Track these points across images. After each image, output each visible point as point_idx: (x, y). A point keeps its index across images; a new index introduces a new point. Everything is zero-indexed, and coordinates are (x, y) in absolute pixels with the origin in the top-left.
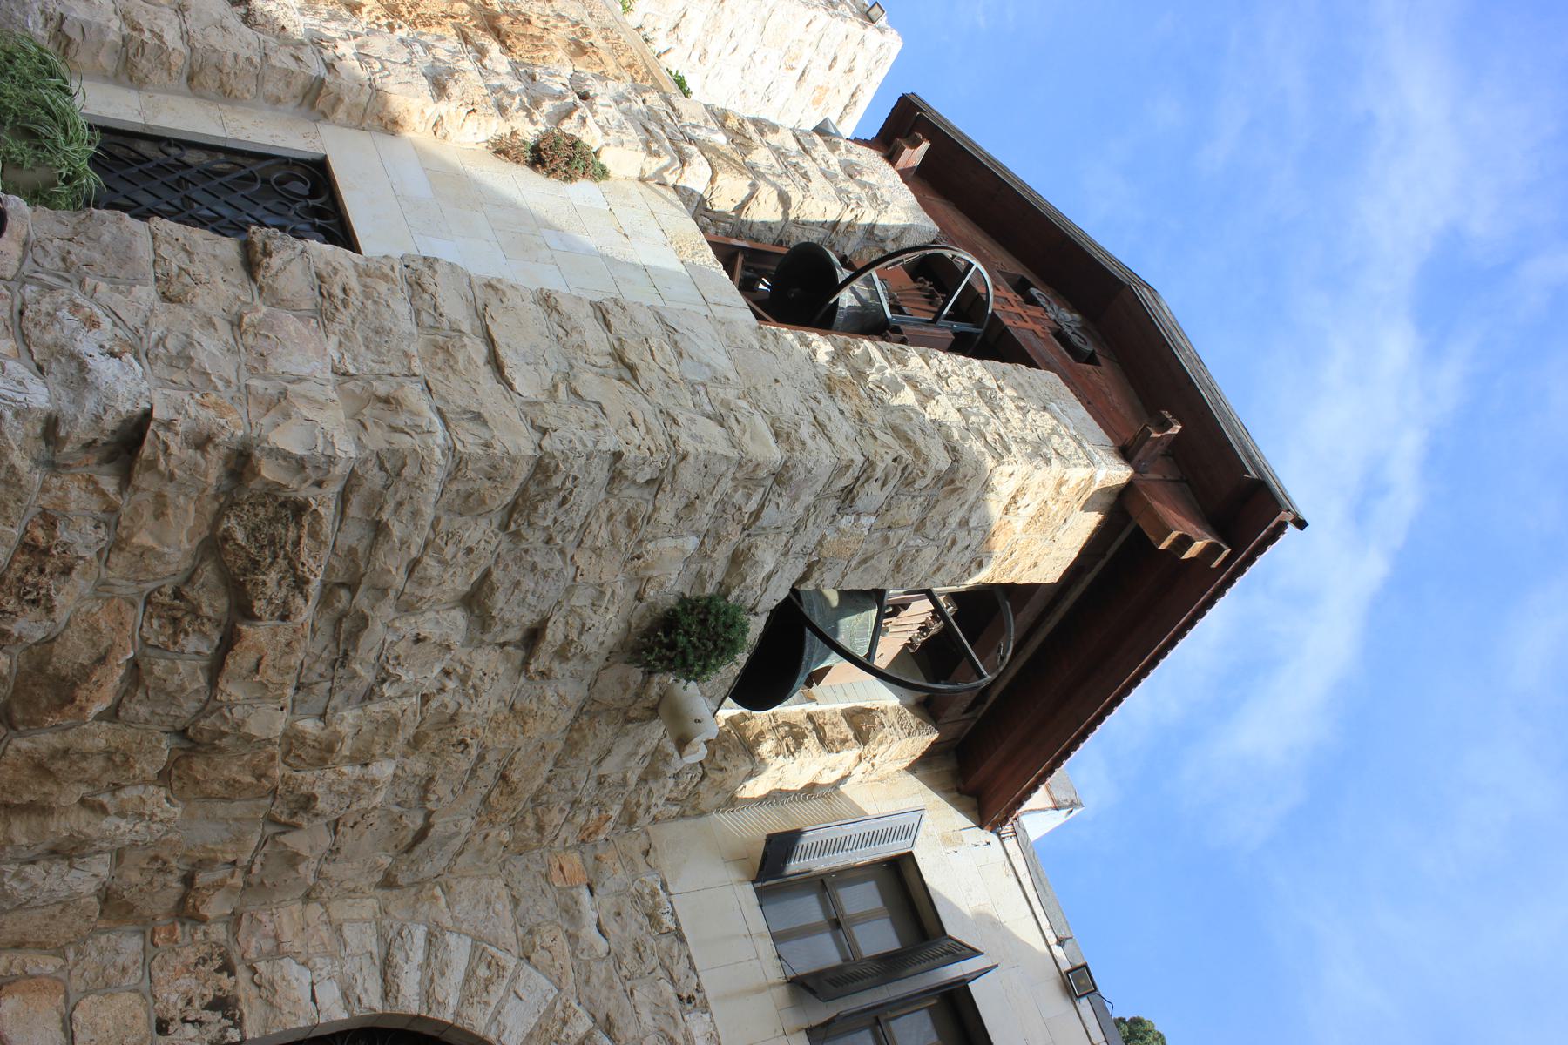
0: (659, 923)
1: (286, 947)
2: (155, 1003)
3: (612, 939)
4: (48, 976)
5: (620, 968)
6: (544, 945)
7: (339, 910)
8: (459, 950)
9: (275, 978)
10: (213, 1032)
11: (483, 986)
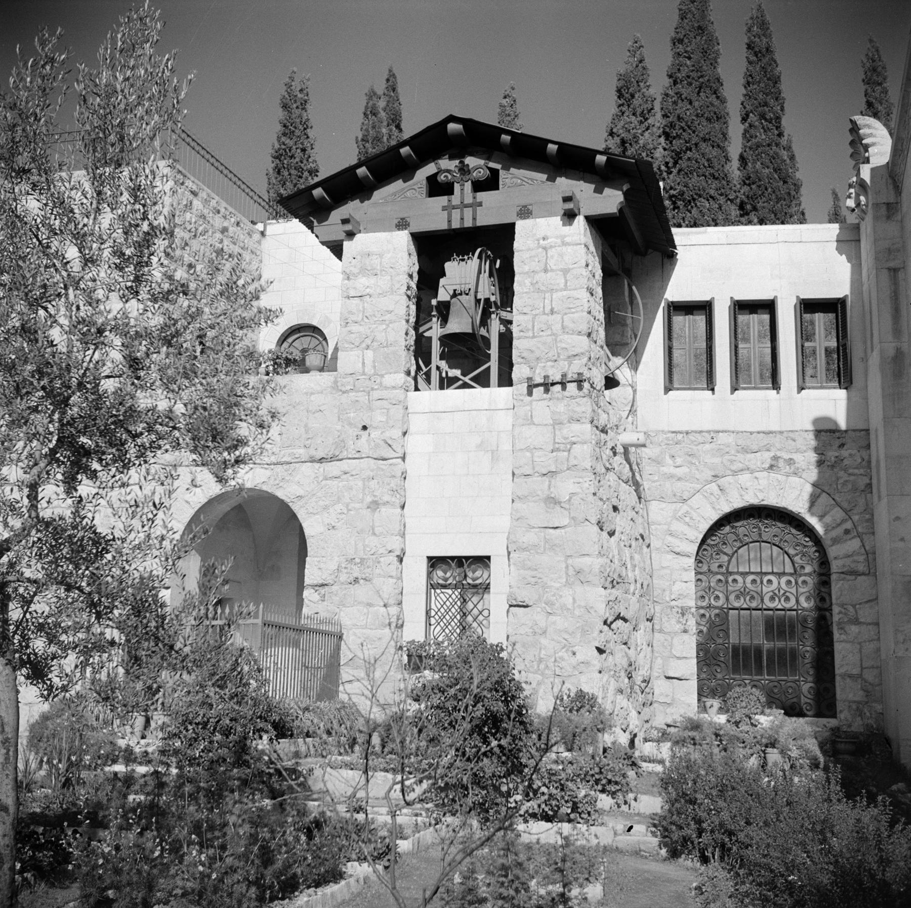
8: (677, 526)
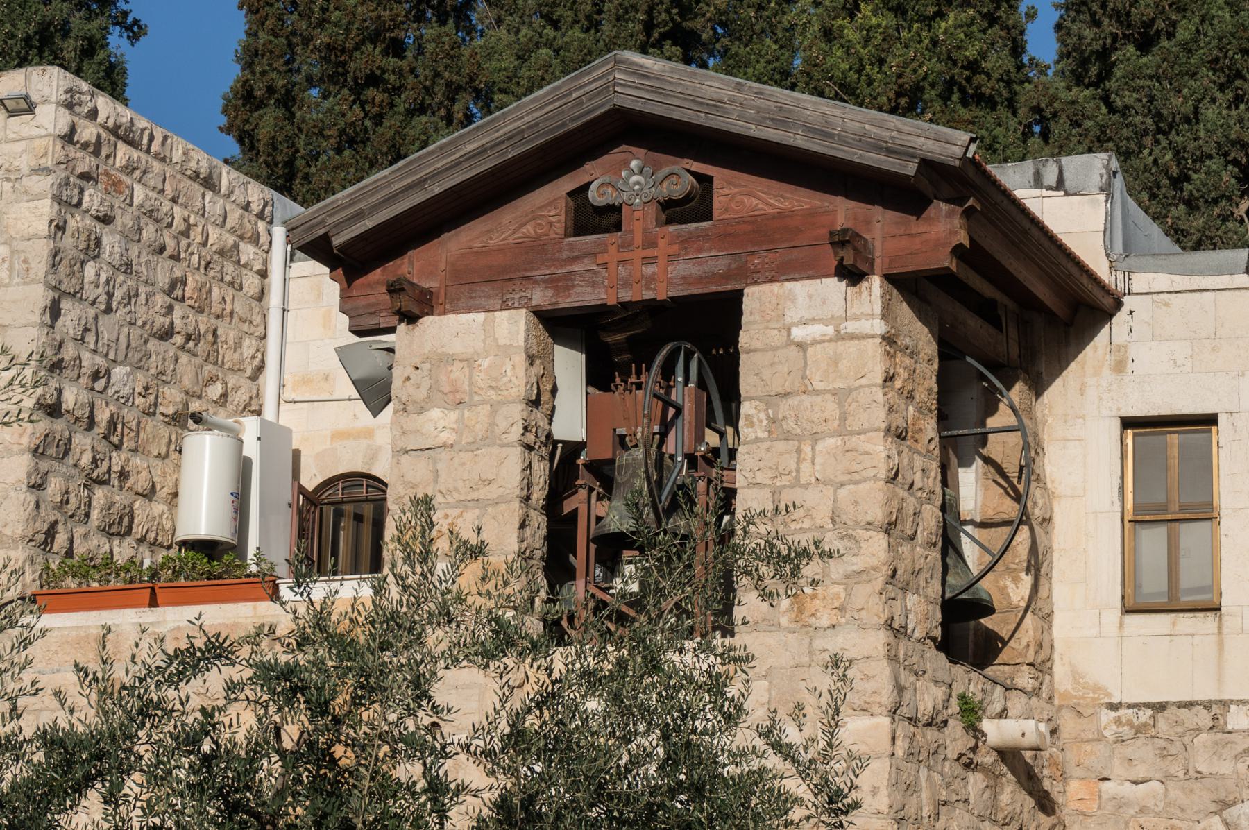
0: (1145, 725)
3: (1151, 775)
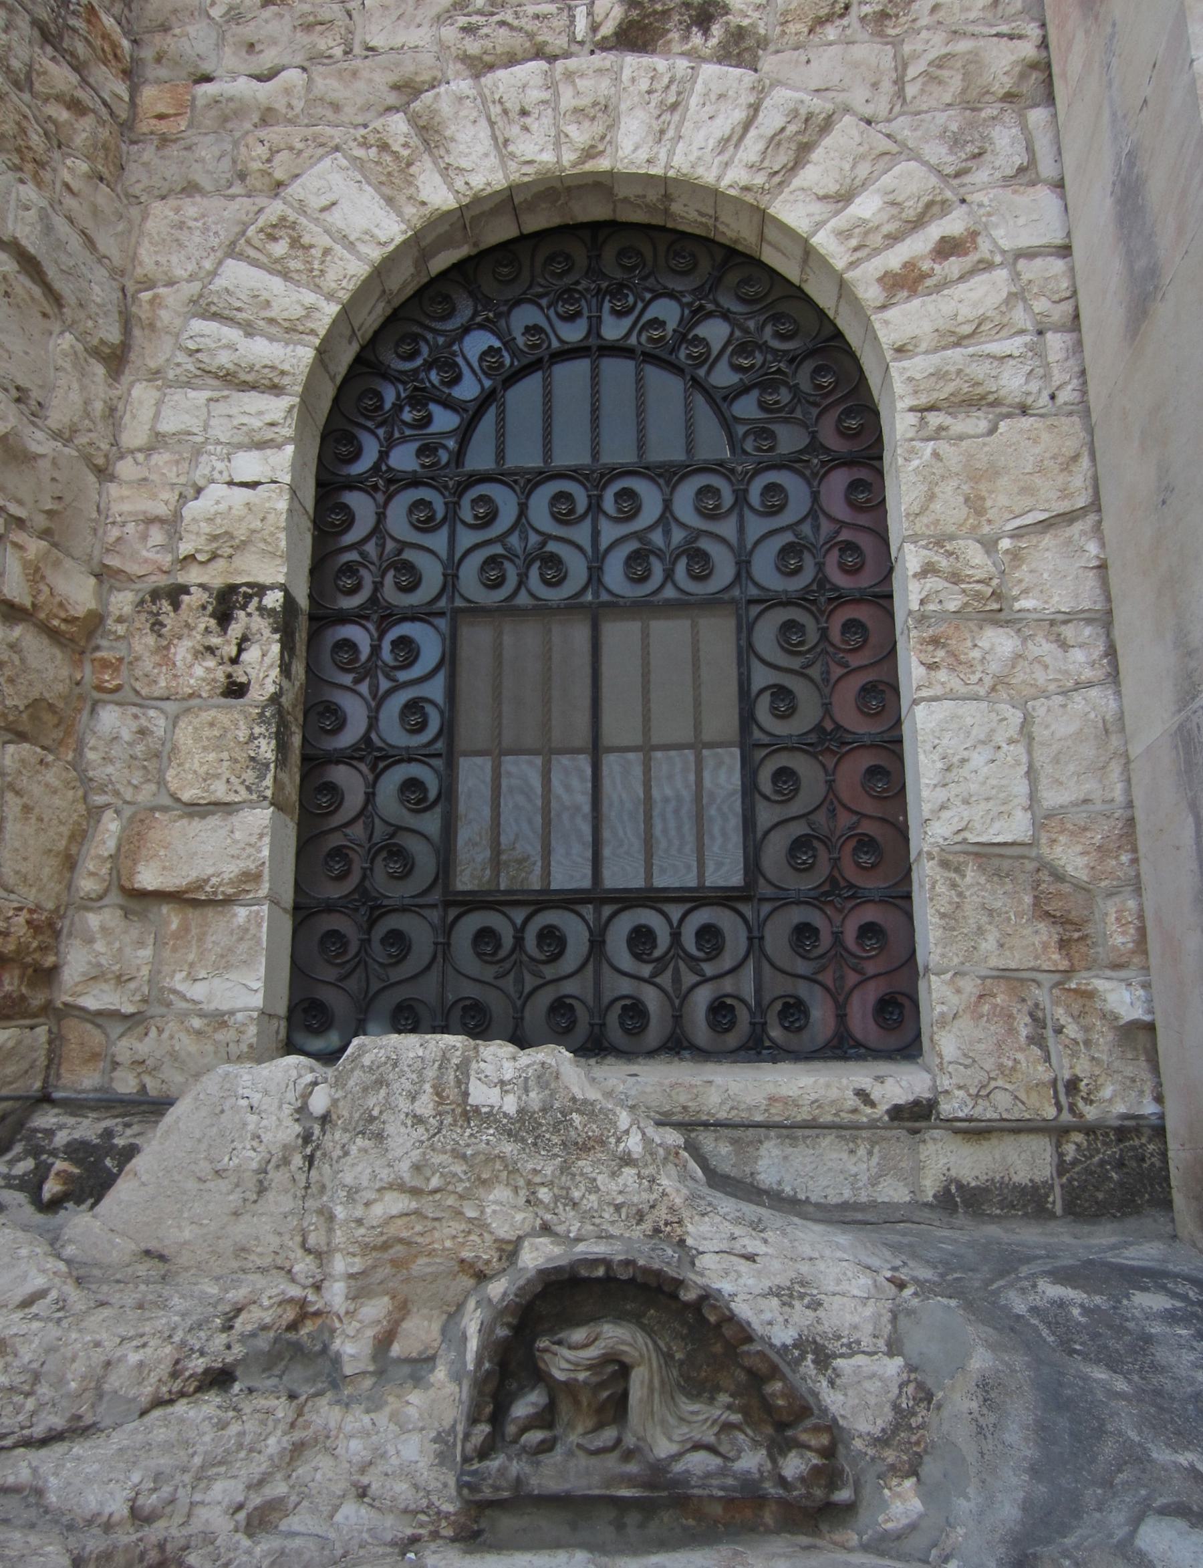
1: (162, 510)
2: (200, 696)
3: (286, 60)
4: (123, 829)
5: (330, 57)
6: (265, 157)
7: (135, 435)
9: (207, 530)
10: (260, 624)
11: (300, 253)
